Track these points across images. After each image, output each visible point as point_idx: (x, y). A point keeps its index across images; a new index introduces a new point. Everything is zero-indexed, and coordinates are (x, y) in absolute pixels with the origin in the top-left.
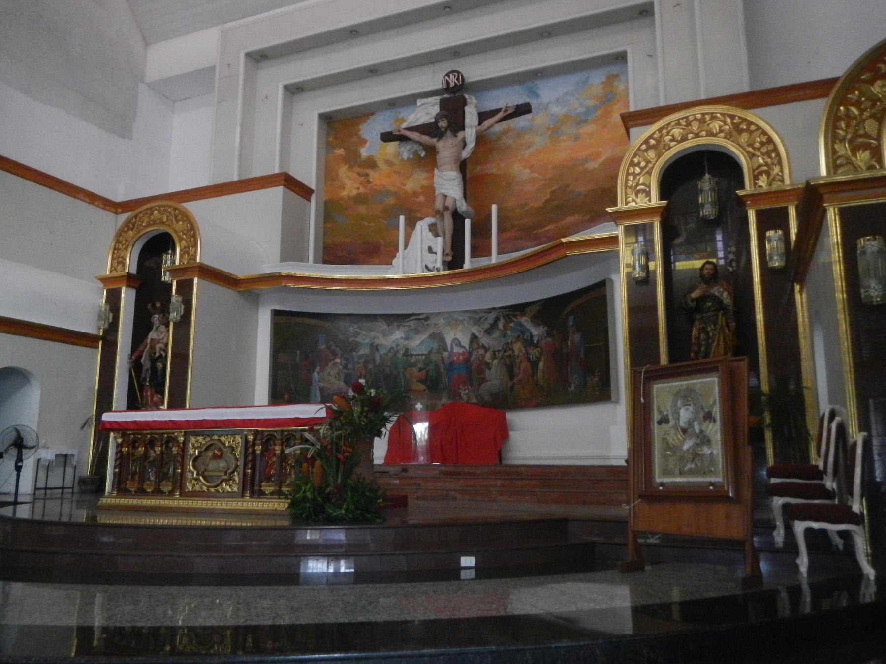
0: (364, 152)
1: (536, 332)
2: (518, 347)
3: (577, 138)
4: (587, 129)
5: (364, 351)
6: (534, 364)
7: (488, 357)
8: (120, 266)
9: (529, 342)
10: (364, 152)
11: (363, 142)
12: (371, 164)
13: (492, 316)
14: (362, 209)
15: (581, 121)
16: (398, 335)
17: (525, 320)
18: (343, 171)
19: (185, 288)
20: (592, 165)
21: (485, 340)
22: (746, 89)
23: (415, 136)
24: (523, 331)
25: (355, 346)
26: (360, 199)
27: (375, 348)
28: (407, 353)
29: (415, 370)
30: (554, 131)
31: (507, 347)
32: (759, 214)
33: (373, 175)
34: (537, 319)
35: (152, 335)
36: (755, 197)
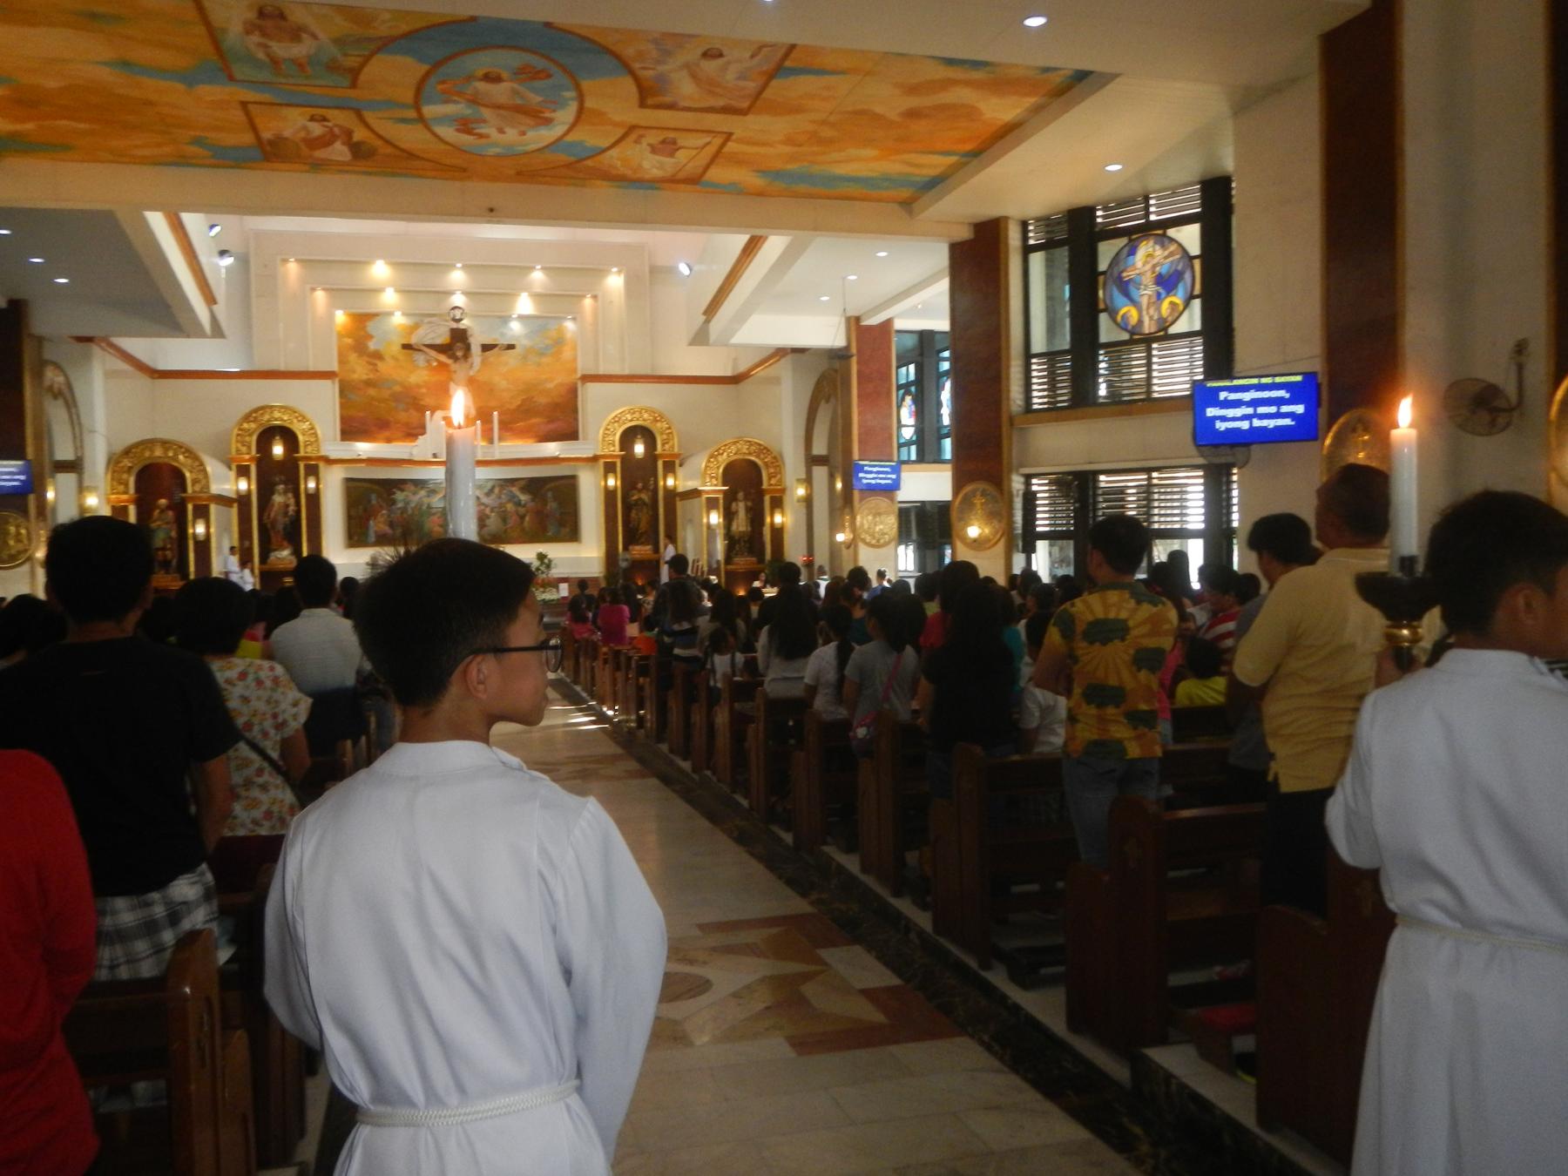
0: (372, 346)
1: (524, 498)
2: (510, 507)
3: (539, 365)
4: (545, 360)
5: (400, 505)
6: (522, 517)
7: (488, 511)
8: (244, 449)
9: (518, 504)
10: (372, 346)
11: (371, 337)
12: (378, 356)
13: (489, 485)
14: (372, 392)
15: (542, 354)
16: (423, 493)
17: (515, 490)
18: (353, 357)
19: (313, 471)
20: (550, 385)
21: (485, 500)
22: (649, 372)
23: (433, 353)
24: (514, 496)
25: (394, 502)
26: (369, 383)
27: (407, 503)
28: (429, 507)
29: (435, 518)
30: (525, 357)
31: (501, 505)
32: (665, 463)
33: (380, 364)
34: (523, 490)
35: (278, 499)
36: (661, 456)
